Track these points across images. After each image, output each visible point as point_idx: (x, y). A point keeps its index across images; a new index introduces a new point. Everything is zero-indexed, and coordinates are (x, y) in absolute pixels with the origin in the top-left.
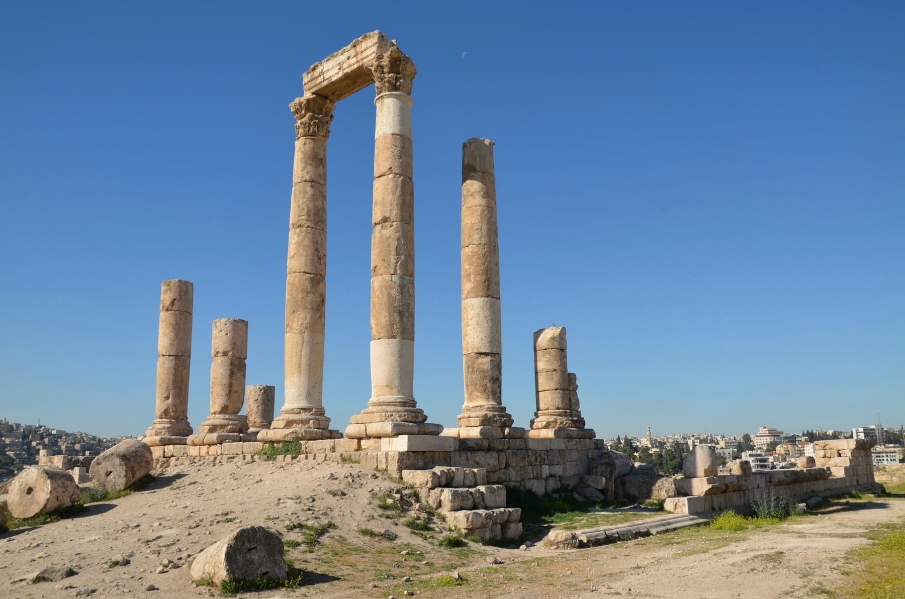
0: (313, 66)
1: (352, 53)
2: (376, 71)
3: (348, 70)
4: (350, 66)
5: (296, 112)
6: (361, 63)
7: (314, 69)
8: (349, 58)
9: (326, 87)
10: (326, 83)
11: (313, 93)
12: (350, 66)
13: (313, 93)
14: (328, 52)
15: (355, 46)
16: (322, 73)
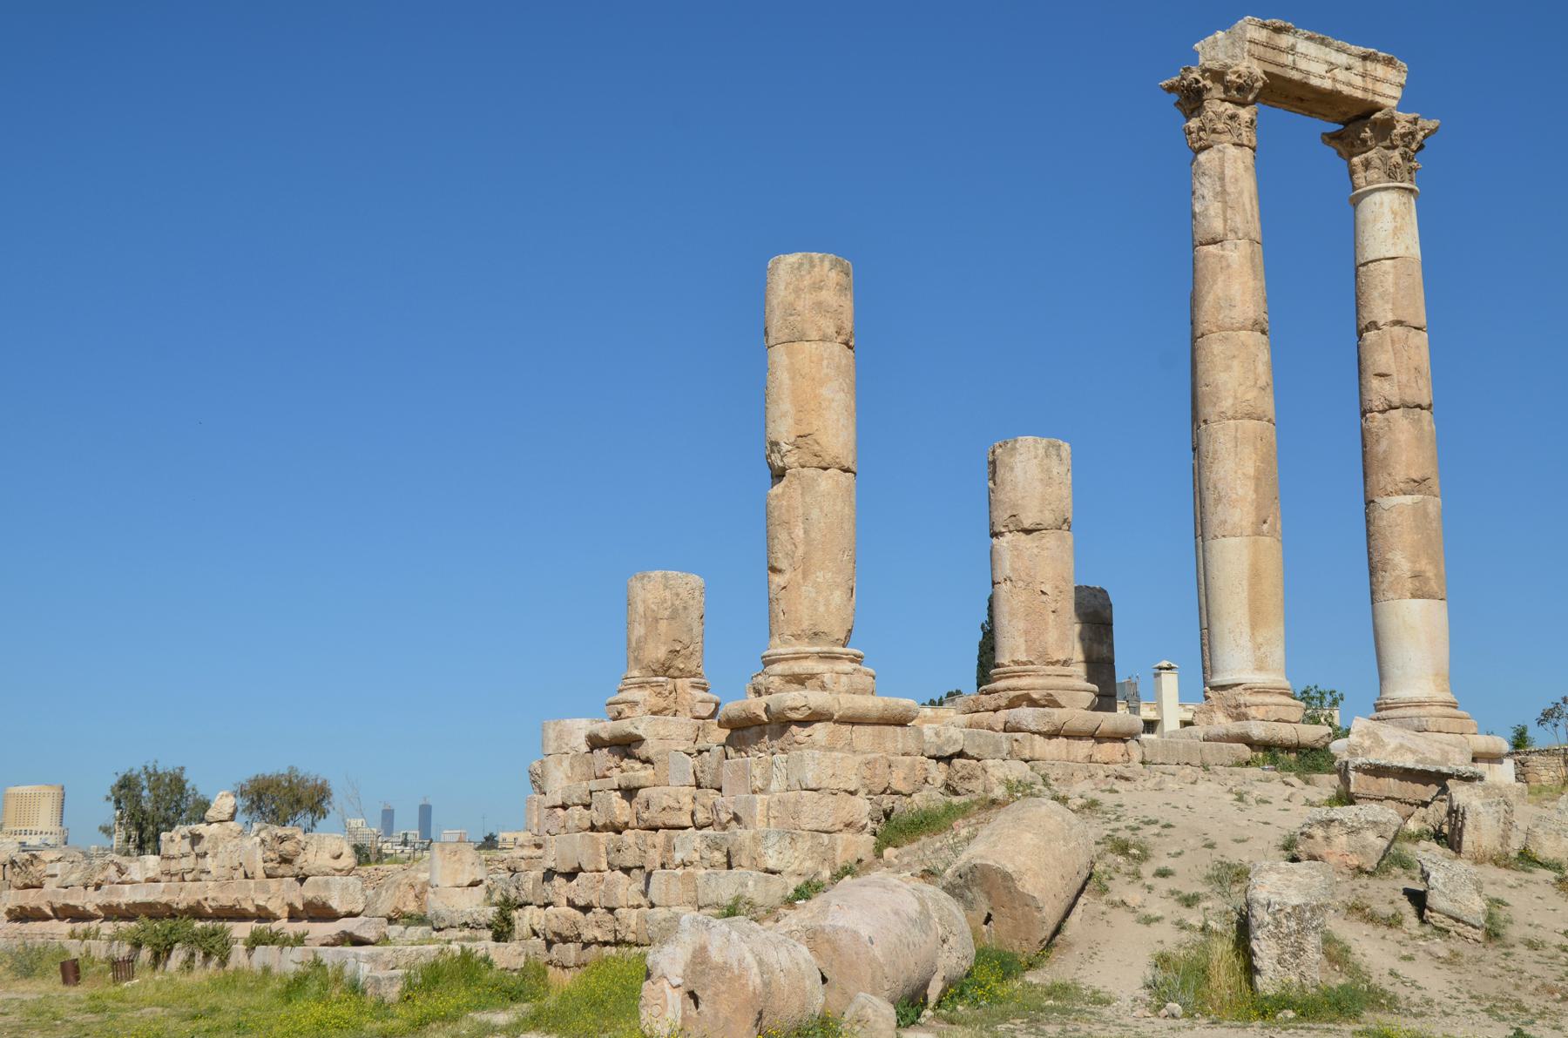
0: (1279, 23)
1: (1358, 65)
2: (1403, 136)
3: (1346, 90)
4: (1349, 84)
5: (1240, 88)
6: (1370, 97)
7: (1278, 30)
8: (1348, 69)
9: (1290, 81)
10: (1296, 76)
11: (1265, 73)
12: (1349, 84)
13: (1265, 73)
14: (1325, 29)
15: (1365, 58)
16: (1292, 49)
